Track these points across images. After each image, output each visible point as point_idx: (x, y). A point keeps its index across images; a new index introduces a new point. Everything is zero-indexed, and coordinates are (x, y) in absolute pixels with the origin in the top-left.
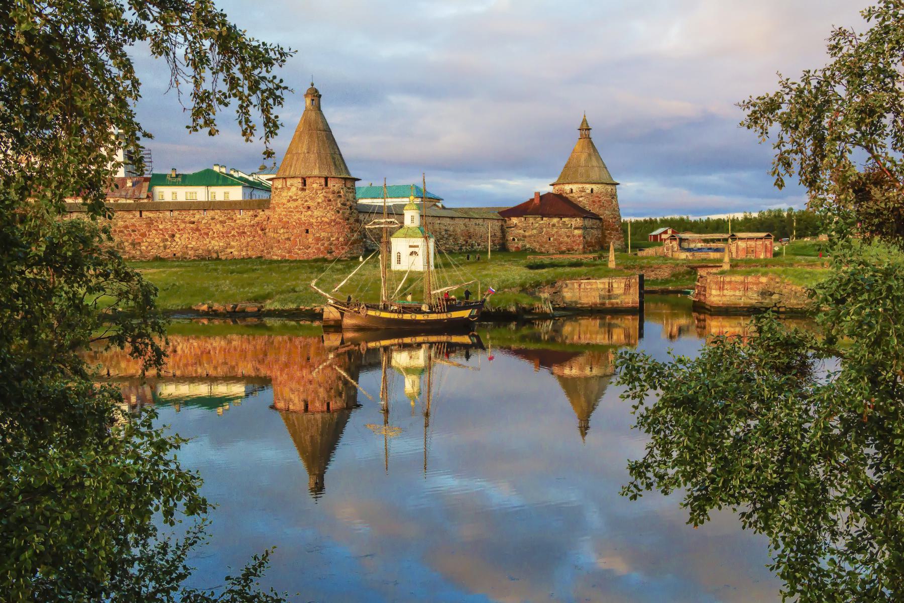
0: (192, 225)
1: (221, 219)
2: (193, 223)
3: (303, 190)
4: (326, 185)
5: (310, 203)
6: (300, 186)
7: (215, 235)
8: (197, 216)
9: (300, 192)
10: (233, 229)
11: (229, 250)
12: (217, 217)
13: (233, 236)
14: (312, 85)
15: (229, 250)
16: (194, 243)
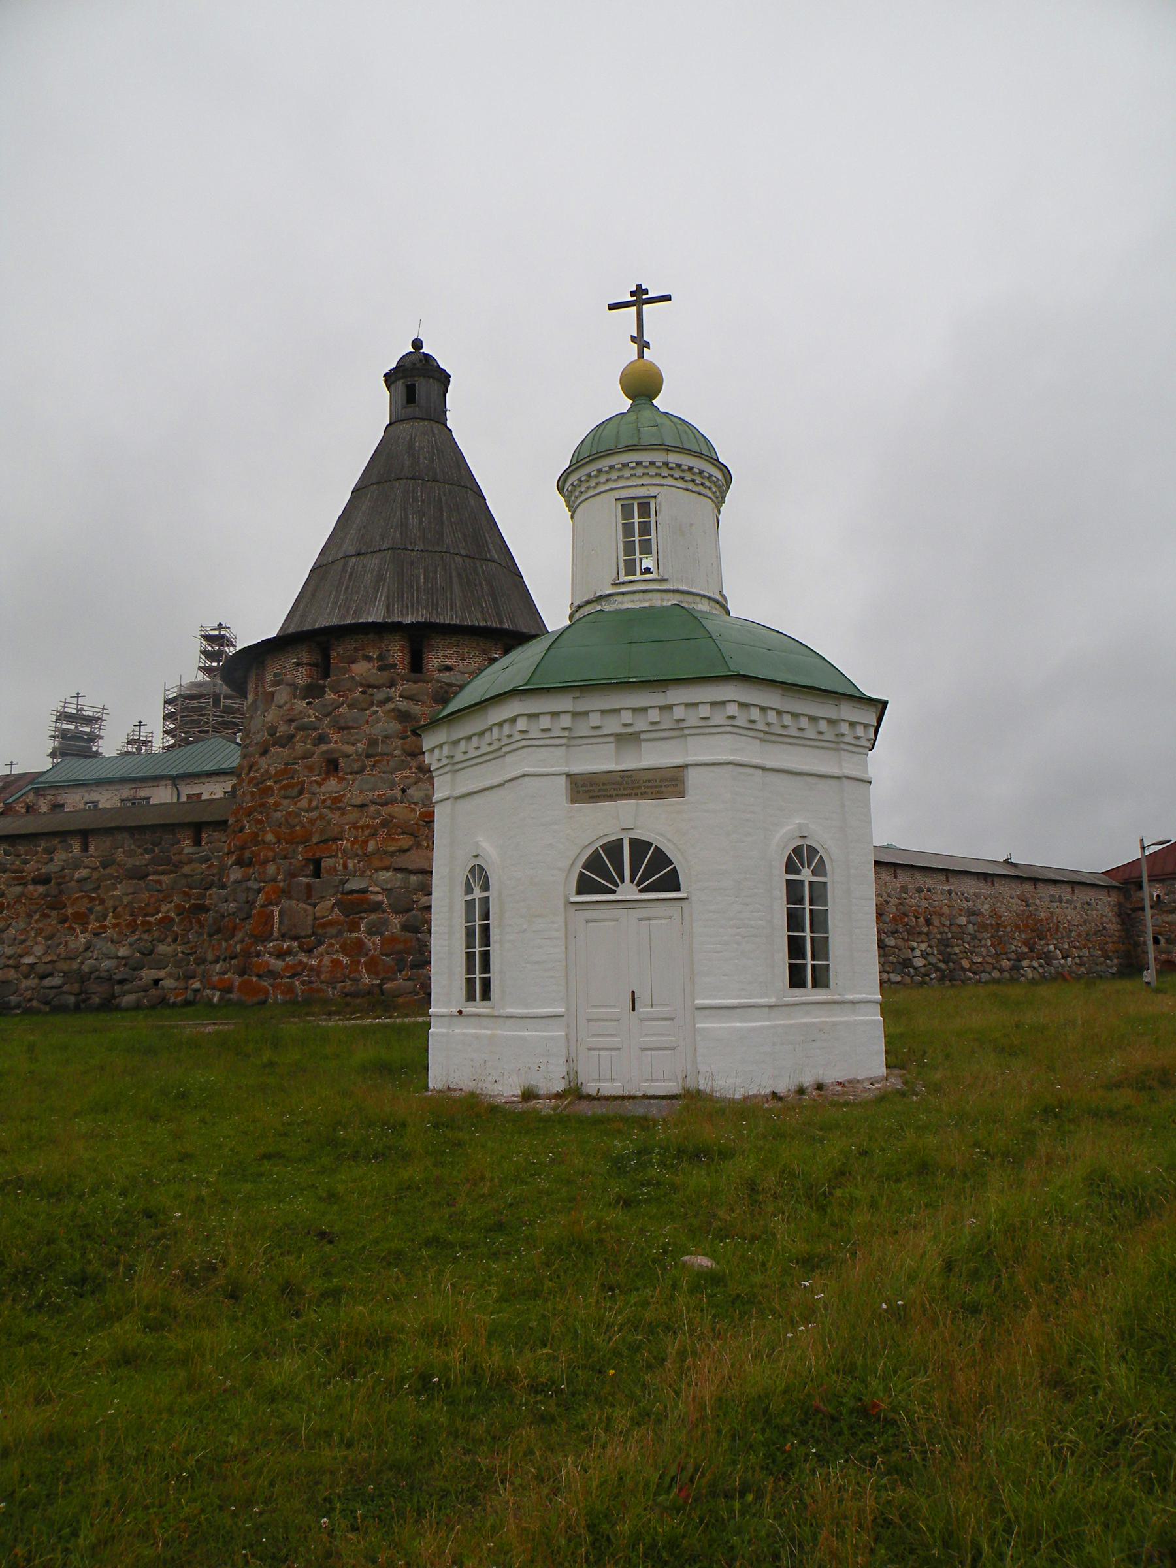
0: (41, 889)
1: (130, 862)
2: (44, 880)
3: (312, 691)
4: (417, 665)
5: (336, 743)
6: (302, 677)
7: (110, 920)
8: (60, 856)
9: (301, 705)
10: (167, 898)
11: (147, 974)
12: (120, 855)
13: (166, 921)
14: (417, 344)
15: (147, 974)
16: (38, 950)
